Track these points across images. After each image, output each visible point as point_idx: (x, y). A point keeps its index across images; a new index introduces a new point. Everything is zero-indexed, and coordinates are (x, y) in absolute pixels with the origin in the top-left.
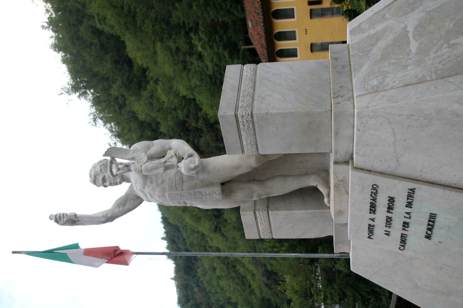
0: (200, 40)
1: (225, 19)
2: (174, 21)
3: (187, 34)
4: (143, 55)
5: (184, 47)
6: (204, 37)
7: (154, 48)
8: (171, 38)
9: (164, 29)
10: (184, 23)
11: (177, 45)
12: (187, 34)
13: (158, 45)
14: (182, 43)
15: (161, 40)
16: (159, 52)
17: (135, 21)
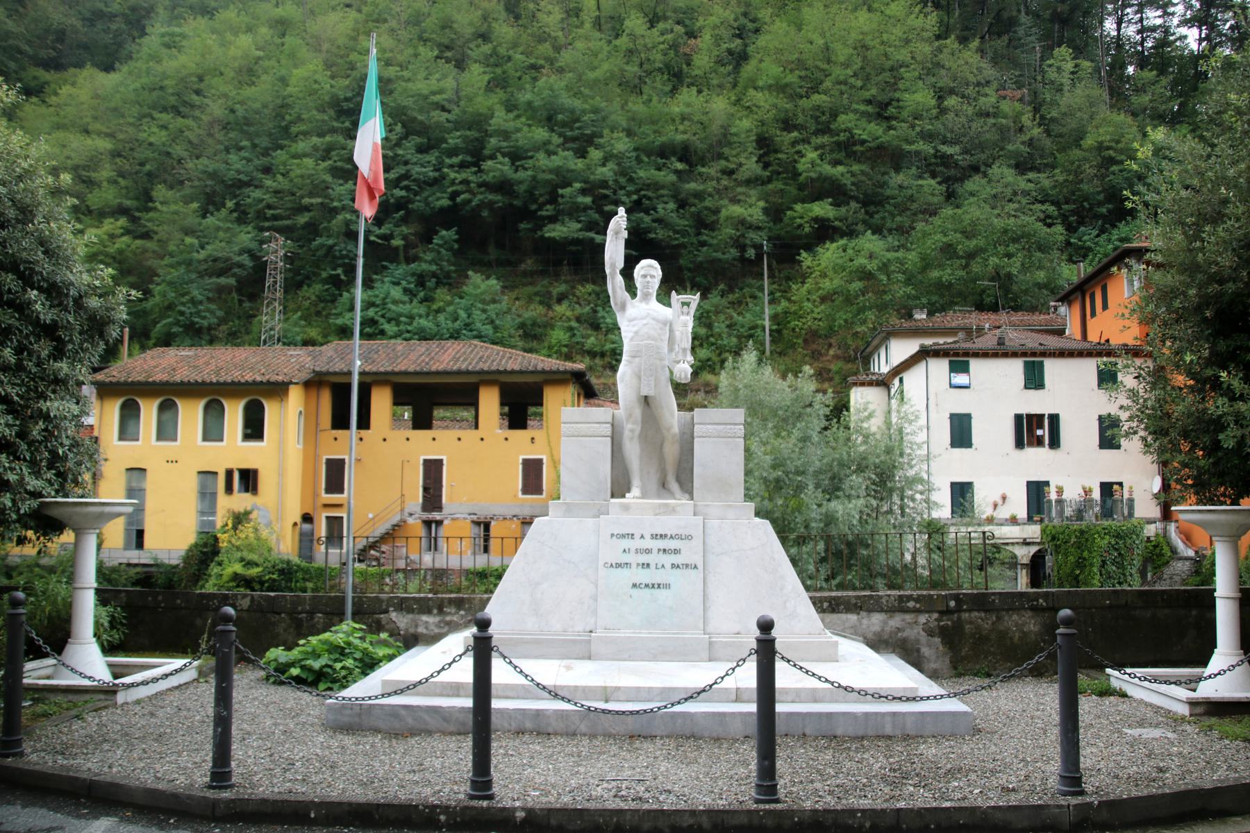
0: (112, 237)
1: (158, 299)
2: (160, 192)
3: (122, 211)
4: (82, 103)
5: (96, 199)
6: (116, 246)
7: (99, 134)
8: (121, 174)
9: (142, 164)
10: (151, 209)
11: (105, 184)
12: (122, 211)
13: (104, 145)
14: (106, 196)
15: (116, 154)
16: (89, 142)
17: (164, 109)
